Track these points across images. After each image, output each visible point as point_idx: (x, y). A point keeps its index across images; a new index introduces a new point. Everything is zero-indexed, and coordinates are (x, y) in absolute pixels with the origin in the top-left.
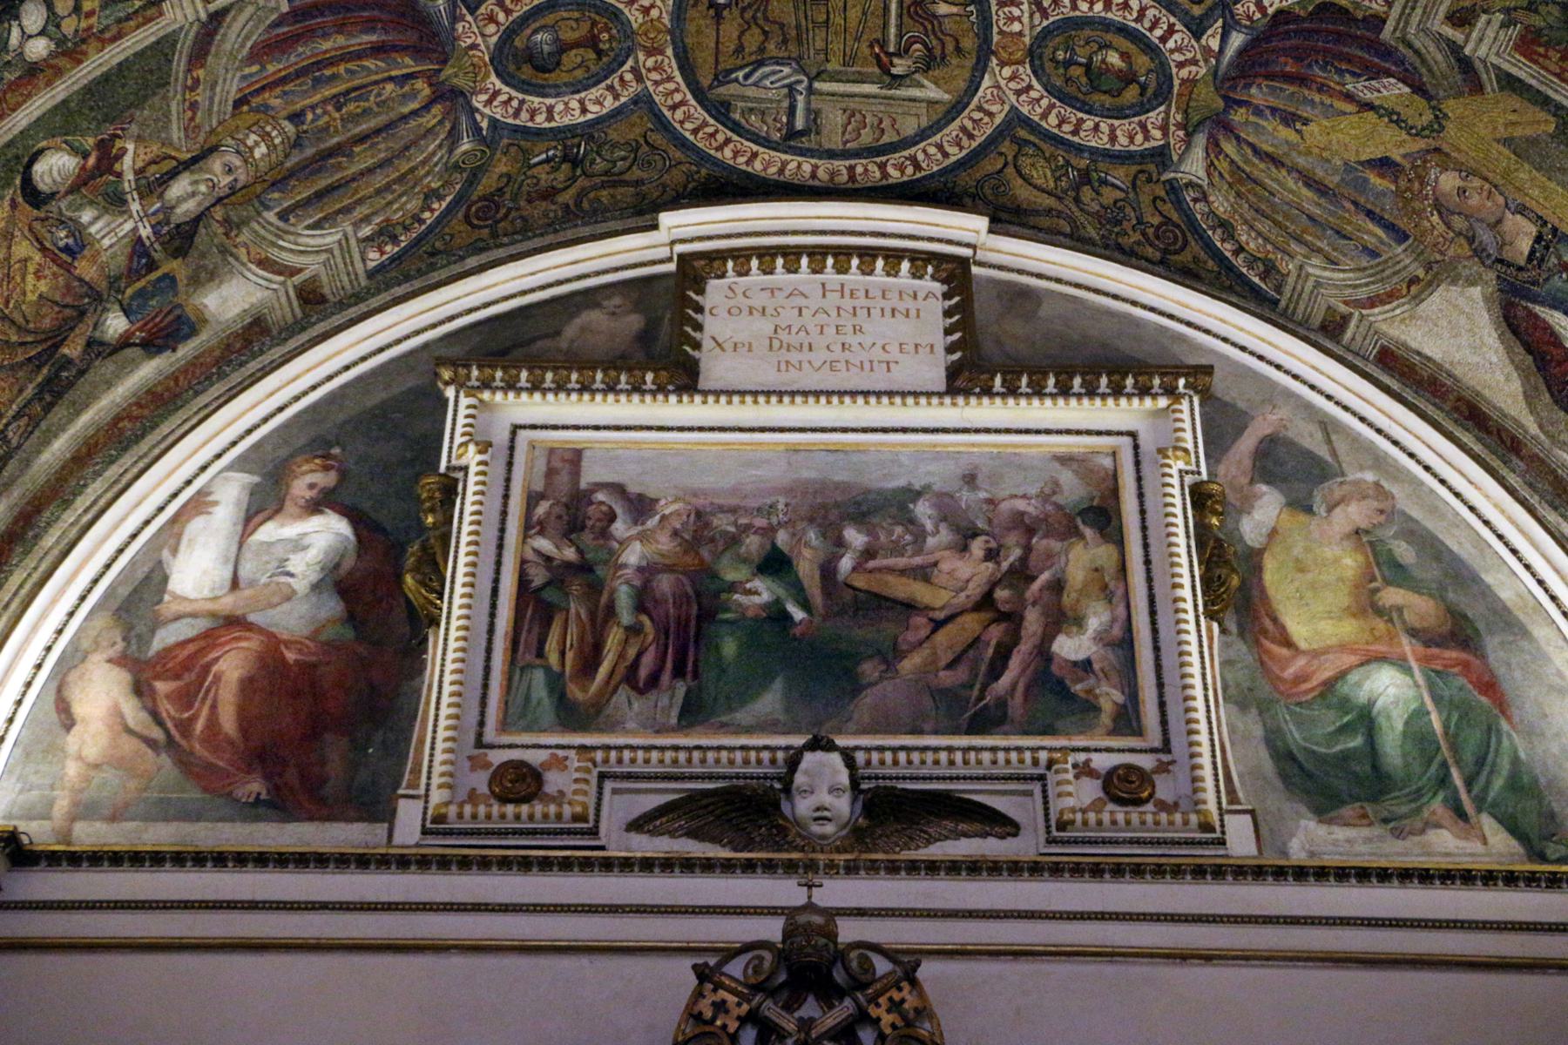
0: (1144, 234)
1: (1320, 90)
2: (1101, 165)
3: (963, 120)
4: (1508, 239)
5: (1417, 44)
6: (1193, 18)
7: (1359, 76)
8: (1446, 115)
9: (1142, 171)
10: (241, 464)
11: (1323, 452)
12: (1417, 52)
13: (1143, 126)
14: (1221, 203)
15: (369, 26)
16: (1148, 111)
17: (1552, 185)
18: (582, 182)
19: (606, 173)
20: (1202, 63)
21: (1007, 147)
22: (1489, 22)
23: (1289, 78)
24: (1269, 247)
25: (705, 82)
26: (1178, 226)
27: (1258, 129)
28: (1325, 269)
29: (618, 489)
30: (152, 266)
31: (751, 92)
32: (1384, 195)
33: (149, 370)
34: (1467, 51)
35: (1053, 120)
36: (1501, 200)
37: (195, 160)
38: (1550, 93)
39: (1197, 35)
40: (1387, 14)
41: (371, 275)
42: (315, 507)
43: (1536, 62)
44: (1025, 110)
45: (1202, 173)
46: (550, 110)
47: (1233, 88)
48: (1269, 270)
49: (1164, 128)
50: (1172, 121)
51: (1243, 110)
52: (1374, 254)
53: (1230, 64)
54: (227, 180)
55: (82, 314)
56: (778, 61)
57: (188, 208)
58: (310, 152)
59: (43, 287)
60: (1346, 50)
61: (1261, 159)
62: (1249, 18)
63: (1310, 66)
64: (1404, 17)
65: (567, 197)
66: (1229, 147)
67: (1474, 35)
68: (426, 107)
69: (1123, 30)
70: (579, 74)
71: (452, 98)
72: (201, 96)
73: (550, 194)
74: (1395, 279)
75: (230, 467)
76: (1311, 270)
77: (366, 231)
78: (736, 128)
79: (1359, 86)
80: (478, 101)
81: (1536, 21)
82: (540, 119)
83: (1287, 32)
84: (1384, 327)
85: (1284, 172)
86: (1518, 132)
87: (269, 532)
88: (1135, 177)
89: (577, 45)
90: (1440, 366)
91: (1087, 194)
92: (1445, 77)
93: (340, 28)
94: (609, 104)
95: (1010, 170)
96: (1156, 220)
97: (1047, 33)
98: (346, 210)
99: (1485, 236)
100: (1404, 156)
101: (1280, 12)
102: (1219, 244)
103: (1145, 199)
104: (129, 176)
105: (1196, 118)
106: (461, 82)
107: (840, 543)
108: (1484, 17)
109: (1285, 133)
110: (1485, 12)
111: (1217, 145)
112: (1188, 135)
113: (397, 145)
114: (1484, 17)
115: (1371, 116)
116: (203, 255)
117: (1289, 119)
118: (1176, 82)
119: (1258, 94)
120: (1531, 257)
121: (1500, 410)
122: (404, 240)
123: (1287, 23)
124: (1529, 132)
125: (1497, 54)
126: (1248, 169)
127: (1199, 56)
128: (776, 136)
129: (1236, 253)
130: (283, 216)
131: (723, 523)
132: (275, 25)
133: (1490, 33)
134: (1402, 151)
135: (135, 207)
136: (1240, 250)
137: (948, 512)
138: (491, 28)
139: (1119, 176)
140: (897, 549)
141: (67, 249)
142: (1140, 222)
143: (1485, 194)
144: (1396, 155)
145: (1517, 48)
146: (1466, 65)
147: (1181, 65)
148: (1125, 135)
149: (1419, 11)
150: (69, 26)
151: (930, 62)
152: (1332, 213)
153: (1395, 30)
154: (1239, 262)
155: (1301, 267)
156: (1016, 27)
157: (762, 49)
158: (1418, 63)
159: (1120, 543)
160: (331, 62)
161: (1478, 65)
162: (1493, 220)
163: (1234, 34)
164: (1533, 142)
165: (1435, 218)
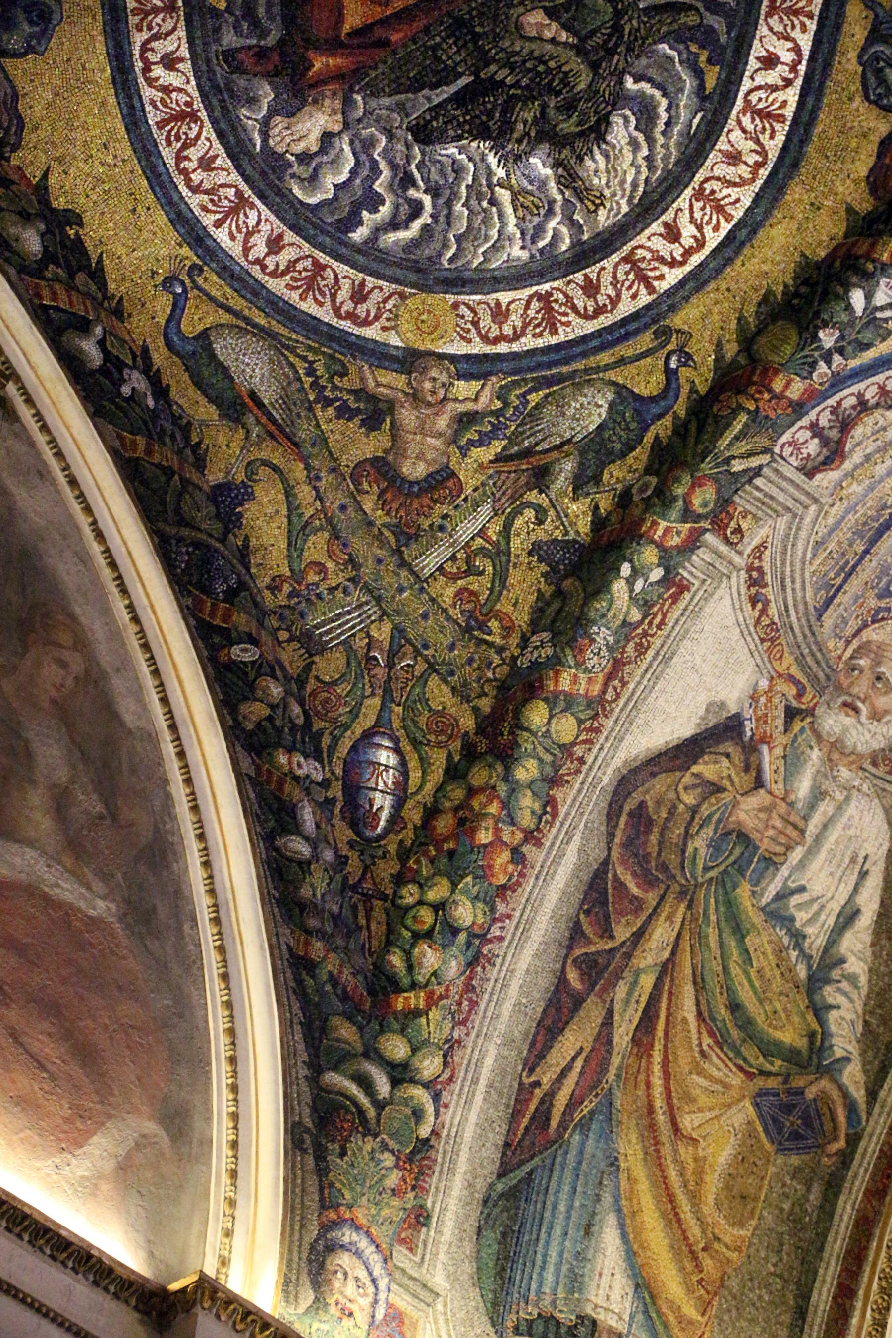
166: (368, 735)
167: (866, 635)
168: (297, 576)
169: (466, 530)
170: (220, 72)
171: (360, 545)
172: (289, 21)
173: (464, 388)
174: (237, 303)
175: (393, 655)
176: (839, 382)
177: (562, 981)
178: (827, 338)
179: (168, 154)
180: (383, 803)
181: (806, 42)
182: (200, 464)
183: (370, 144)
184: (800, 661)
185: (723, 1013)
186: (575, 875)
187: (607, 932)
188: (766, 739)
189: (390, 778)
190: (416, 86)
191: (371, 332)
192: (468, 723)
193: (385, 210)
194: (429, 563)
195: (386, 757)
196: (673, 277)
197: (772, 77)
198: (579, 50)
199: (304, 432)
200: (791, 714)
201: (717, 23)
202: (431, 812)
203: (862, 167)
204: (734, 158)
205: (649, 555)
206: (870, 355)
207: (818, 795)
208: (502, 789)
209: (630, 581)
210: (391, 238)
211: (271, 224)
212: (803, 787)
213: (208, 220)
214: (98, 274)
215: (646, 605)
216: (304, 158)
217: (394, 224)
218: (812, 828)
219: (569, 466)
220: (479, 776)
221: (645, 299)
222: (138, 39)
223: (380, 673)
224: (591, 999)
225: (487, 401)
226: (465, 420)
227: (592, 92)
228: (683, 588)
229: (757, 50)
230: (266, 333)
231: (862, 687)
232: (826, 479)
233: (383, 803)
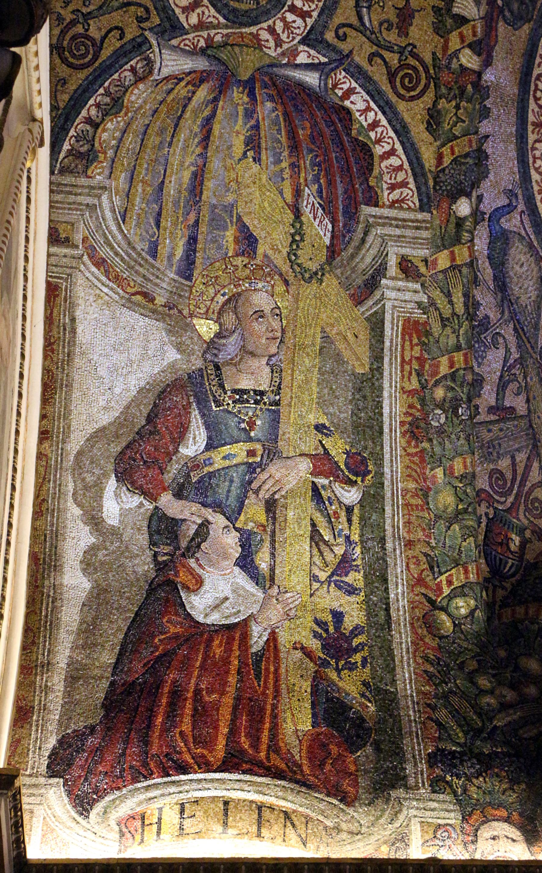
0: (73, 23)
1: (293, 166)
4: (242, 366)
5: (370, 239)
6: (322, 33)
7: (321, 197)
8: (321, 281)
9: (147, 10)
12: (363, 241)
16: (214, 6)
17: (315, 389)
20: (279, 50)
22: (416, 292)
23: (292, 135)
24: (110, 153)
26: (96, 57)
27: (234, 116)
28: (113, 211)
32: (220, 247)
34: (384, 281)
36: (273, 350)
38: (386, 360)
39: (304, 41)
40: (384, 205)
43: (403, 339)
45: (166, 72)
47: (265, 86)
49: (201, 26)
50: (212, 32)
51: (246, 99)
52: (154, 252)
53: (287, 78)
60: (338, 180)
61: (203, 126)
62: (335, 86)
63: (311, 151)
64: (388, 221)
67: (400, 283)
74: (139, 280)
76: (105, 198)
79: (312, 199)
81: (436, 328)
83: (333, 123)
84: (80, 281)
85: (198, 150)
86: (341, 346)
88: (139, 5)
90: (72, 342)
92: (353, 270)
96: (95, 33)
100: (265, 256)
101: (348, 112)
102: (91, 102)
105: (223, 56)
108: (418, 286)
110: (422, 285)
111: (202, 81)
112: (203, 52)
114: (418, 286)
115: (289, 216)
118: (253, 29)
120: (235, 391)
121: (67, 413)
123: (340, 120)
124: (346, 354)
125: (394, 307)
126: (188, 115)
127: (285, 46)
129: (89, 120)
133: (408, 296)
134: (270, 252)
142: (87, 16)
143: (271, 335)
144: (261, 250)
145: (407, 321)
147: (272, 30)
149: (398, 232)
152: (176, 203)
153: (375, 217)
155: (104, 188)
158: (355, 243)
161: (377, 295)
162: (250, 348)
163: (316, 75)
164: (338, 358)
165: (221, 300)
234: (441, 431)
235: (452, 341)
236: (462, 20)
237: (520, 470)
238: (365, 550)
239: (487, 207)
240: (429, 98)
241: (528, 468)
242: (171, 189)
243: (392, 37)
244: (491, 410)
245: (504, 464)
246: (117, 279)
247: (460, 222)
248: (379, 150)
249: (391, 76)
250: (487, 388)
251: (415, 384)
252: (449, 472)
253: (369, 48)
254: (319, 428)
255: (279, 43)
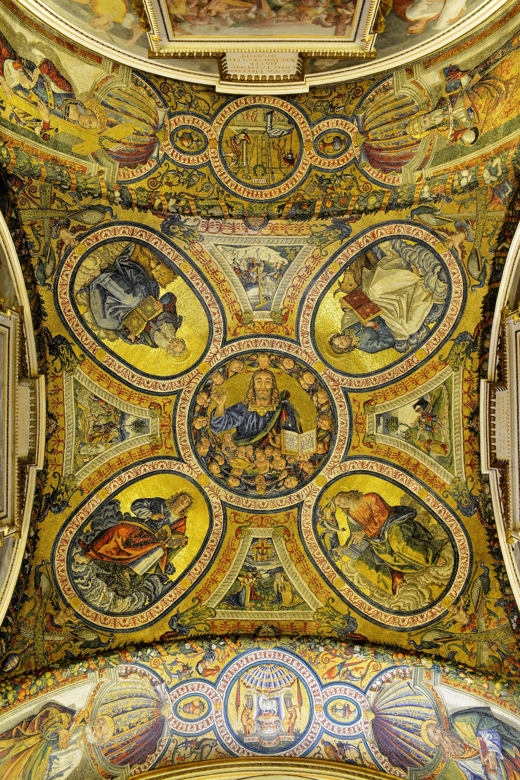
2: (186, 109)
3: (225, 120)
10: (437, 32)
11: (113, 36)
13: (176, 124)
14: (152, 103)
15: (382, 158)
18: (330, 99)
19: (323, 102)
21: (212, 112)
23: (140, 146)
25: (295, 130)
29: (323, 26)
30: (451, 97)
31: (282, 127)
33: (459, 60)
35: (200, 123)
37: (433, 128)
39: (165, 154)
41: (392, 75)
42: (417, 22)
44: (208, 125)
46: (337, 125)
48: (136, 83)
49: (170, 124)
52: (109, 95)
54: (426, 119)
55: (472, 88)
56: (275, 137)
57: (438, 113)
58: (403, 122)
59: (480, 102)
64: (115, 170)
65: (335, 94)
66: (153, 121)
68: (370, 130)
69: (184, 152)
70: (328, 135)
71: (364, 132)
72: (428, 147)
73: (340, 96)
75: (440, 31)
77: (391, 92)
78: (287, 115)
80: (356, 130)
81: (83, 177)
82: (340, 122)
84: (102, 71)
86: (81, 145)
87: (432, 15)
89: (329, 144)
91: (189, 100)
93: (390, 158)
94: (321, 125)
95: (211, 105)
96: (169, 93)
97: (204, 149)
98: (396, 100)
99: (82, 110)
103: (173, 100)
104: (451, 128)
106: (361, 136)
107: (256, 14)
109: (138, 129)
113: (379, 118)
116: (437, 96)
117: (138, 133)
119: (147, 139)
122: (381, 86)
124: (78, 146)
128: (276, 112)
130: (413, 102)
131: (292, 18)
132: (405, 163)
135: (451, 118)
136: (145, 88)
137: (224, 22)
138: (351, 152)
139: (181, 108)
140: (238, 13)
141: (472, 111)
146: (97, 160)
148: (181, 120)
150: (456, 177)
151: (234, 138)
154: (145, 83)
156: (212, 150)
157: (279, 141)
159: (170, 14)
160: (393, 149)
164: (76, 143)
166: (16, 654)
167: (106, 717)
168: (25, 620)
169: (57, 638)
170: (77, 541)
171: (38, 625)
172: (92, 543)
173: (75, 618)
174: (50, 573)
175: (30, 646)
176: (136, 663)
177: (12, 730)
178: (140, 653)
179: (59, 544)
180: (9, 667)
181: (165, 609)
182: (26, 589)
183: (88, 570)
184: (92, 711)
185: (28, 771)
186: (30, 712)
187: (25, 729)
188: (76, 721)
189: (14, 665)
190: (102, 568)
191: (66, 597)
192: (33, 668)
193: (83, 581)
194: (47, 638)
195: (16, 660)
196: (120, 627)
197: (156, 610)
198: (130, 583)
199: (45, 600)
200: (83, 720)
201: (153, 596)
202: (16, 677)
203: (161, 633)
204: (142, 617)
205: (86, 665)
206: (144, 663)
207: (75, 741)
208: (33, 682)
209: (80, 667)
210: (80, 586)
211: (65, 567)
212: (74, 738)
213: (56, 558)
214: (35, 549)
215: (79, 674)
216: (77, 563)
217: (83, 584)
218: (70, 748)
219: (81, 643)
220: (30, 676)
221: (113, 627)
222: (69, 525)
223: (26, 647)
224: (13, 740)
225: (76, 622)
226: (70, 622)
227: (127, 591)
228: (86, 677)
229: (156, 604)
230: (50, 581)
231: (97, 727)
232: (122, 679)
233: (9, 667)
234: (54, 169)
235: (80, 181)
236: (168, 201)
237: (35, 200)
238: (22, 129)
239: (114, 207)
240: (147, 189)
241: (35, 203)
242: (127, 105)
243: (165, 180)
244: (55, 194)
245: (38, 194)
246: (102, 82)
247: (113, 192)
248: (134, 171)
249: (154, 178)
250: (62, 194)
251: (68, 165)
252: (42, 166)
253: (162, 173)
254: (57, 130)
255: (165, 146)
